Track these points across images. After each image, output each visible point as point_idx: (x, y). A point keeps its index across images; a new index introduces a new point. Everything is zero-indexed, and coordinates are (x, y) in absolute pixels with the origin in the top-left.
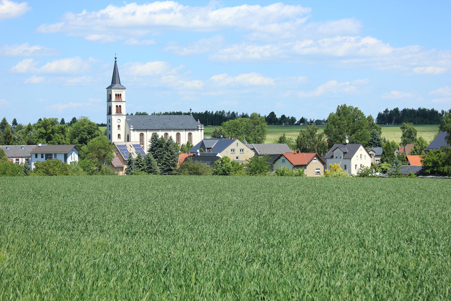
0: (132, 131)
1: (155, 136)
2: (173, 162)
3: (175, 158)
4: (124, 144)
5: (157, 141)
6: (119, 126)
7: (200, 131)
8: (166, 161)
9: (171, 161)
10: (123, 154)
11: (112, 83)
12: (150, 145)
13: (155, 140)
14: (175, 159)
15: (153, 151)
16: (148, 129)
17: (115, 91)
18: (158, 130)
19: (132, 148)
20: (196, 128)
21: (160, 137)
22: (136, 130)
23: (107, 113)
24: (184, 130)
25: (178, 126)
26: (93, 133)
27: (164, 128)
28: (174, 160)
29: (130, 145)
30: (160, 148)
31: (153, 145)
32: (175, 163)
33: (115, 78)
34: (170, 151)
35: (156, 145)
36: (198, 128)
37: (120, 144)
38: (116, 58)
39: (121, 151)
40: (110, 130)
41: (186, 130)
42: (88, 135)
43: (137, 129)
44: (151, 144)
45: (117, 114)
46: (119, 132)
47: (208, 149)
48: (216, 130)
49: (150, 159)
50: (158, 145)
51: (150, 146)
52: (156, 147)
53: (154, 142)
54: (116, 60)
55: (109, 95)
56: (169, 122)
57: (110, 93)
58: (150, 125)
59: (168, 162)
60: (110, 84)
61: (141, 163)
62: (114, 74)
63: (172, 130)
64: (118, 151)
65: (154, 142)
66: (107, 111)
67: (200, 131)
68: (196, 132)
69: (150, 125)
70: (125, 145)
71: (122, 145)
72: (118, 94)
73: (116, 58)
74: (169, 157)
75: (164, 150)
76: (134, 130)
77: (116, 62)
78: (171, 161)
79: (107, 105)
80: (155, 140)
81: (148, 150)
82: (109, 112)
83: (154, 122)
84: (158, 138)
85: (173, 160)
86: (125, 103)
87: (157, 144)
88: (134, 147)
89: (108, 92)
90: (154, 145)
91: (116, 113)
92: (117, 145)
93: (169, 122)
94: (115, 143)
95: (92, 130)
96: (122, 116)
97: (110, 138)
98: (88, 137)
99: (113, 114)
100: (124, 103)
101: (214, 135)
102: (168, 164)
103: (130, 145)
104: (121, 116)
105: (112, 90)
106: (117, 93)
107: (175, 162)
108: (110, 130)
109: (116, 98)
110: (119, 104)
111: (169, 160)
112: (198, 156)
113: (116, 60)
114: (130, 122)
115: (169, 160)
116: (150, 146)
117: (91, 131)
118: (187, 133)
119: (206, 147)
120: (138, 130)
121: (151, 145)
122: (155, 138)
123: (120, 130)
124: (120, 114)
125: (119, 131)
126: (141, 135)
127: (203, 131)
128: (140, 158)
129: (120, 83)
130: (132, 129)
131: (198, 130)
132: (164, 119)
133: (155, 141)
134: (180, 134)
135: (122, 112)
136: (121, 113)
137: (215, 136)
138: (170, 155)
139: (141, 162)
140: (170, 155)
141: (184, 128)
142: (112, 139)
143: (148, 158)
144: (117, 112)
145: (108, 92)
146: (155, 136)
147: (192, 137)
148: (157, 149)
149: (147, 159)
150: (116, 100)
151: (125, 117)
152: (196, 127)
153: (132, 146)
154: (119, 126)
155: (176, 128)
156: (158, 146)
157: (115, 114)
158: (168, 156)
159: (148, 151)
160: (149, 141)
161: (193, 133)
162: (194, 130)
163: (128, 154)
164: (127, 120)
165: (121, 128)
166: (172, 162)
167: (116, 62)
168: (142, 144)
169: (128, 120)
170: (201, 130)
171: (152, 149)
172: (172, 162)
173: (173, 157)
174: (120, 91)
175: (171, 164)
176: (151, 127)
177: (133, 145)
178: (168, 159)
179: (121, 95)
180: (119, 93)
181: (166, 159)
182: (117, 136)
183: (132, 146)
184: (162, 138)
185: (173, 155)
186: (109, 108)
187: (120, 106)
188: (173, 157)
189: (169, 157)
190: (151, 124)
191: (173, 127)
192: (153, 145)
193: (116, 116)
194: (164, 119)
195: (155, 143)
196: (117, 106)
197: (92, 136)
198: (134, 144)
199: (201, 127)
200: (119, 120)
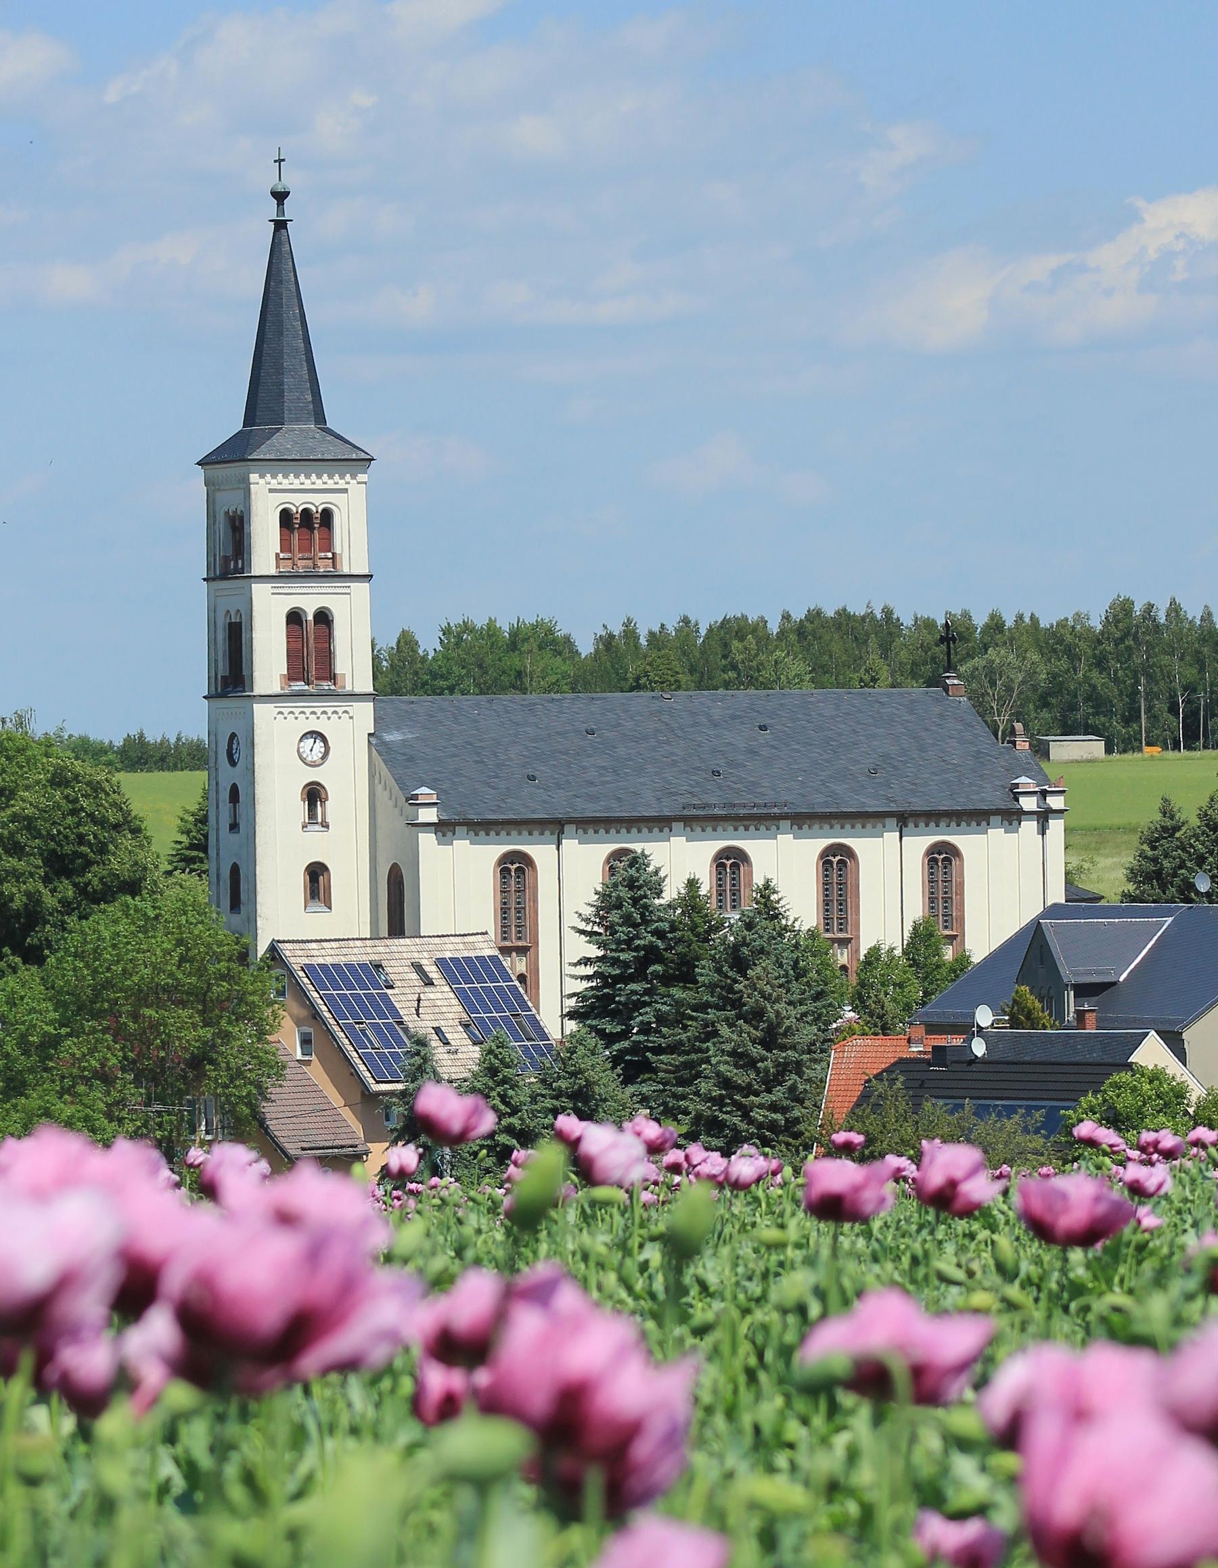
0: (427, 840)
1: (631, 884)
2: (784, 1110)
3: (800, 1074)
4: (365, 959)
5: (646, 922)
6: (314, 795)
7: (1029, 827)
8: (719, 1102)
9: (766, 1098)
10: (357, 1044)
11: (249, 419)
12: (586, 961)
13: (628, 920)
14: (801, 1087)
15: (613, 1015)
16: (571, 821)
17: (274, 484)
18: (661, 824)
19: (430, 994)
20: (999, 800)
21: (672, 890)
22: (461, 830)
23: (213, 678)
24: (891, 822)
25: (839, 788)
26: (89, 863)
27: (714, 800)
28: (793, 1088)
29: (418, 968)
30: (677, 992)
31: (615, 962)
32: (797, 1121)
33: (280, 371)
34: (757, 1015)
35: (643, 963)
36: (1011, 805)
37: (329, 961)
38: (280, 197)
39: (337, 1014)
40: (234, 827)
41: (905, 820)
42: (46, 880)
43: (475, 817)
44: (594, 952)
45: (299, 686)
46: (316, 847)
47: (1083, 991)
48: (1169, 823)
49: (589, 1084)
50: (660, 960)
51: (589, 971)
52: (640, 975)
53: (623, 932)
54: (281, 211)
55: (221, 518)
56: (752, 752)
57: (229, 502)
58: (591, 783)
59: (739, 1106)
60: (238, 426)
61: (514, 1121)
62: (269, 335)
63: (785, 824)
64: (316, 1015)
65: (623, 932)
66: (213, 663)
67: (1029, 827)
68: (996, 834)
69: (591, 783)
70: (378, 966)
71: (350, 966)
72: (306, 512)
73: (280, 197)
74: (749, 1063)
75: (703, 1007)
76: (444, 829)
77: (280, 225)
78: (766, 1098)
79: (212, 610)
80: (628, 920)
81: (572, 1003)
82: (223, 669)
83: (621, 751)
84: (657, 902)
85: (779, 1094)
86: (365, 586)
87: (652, 954)
88: (451, 979)
89: (219, 496)
90: (626, 965)
91: (291, 677)
92: (309, 969)
93: (752, 752)
94: (287, 950)
95: (81, 839)
96: (341, 706)
97: (235, 904)
98: (50, 901)
99: (259, 688)
100: (355, 586)
101: (1155, 860)
102: (734, 1129)
103: (418, 968)
104: (329, 706)
105: (254, 477)
106: (298, 502)
107: (796, 1113)
108: (234, 827)
109: (285, 545)
110: (309, 600)
111: (748, 1090)
112: (975, 1060)
113: (281, 211)
114: (411, 759)
115: (748, 1090)
116: (589, 971)
117: (68, 849)
118: (918, 844)
119: (1068, 974)
120: (481, 828)
121: (599, 959)
122: (635, 901)
123: (325, 825)
124: (326, 685)
125: (315, 835)
126: (505, 872)
127: (1056, 826)
128: (505, 1081)
129: (320, 418)
130: (429, 815)
131: (1012, 817)
132: (715, 725)
133: (635, 926)
134: (848, 852)
135: (341, 666)
136: (332, 677)
137: (1158, 875)
138: (756, 1051)
139: (515, 1111)
140: (756, 1051)
141: (893, 808)
142: (260, 909)
143: (573, 1074)
144: (297, 669)
145: (219, 496)
146: (631, 884)
147: (961, 885)
148: (647, 992)
149: (563, 1084)
150: (286, 568)
151: (365, 713)
152: (993, 798)
153: (433, 972)
154: (314, 795)
155: (819, 802)
156: (658, 968)
157: (276, 689)
158: (741, 1059)
159: (572, 1015)
160: (582, 926)
161: (967, 843)
162: (977, 818)
163: (401, 1043)
164: (388, 738)
165: (332, 809)
166: (773, 1107)
167: (280, 225)
168: (522, 951)
169: (393, 737)
170: (1044, 817)
171: (609, 999)
172: (773, 1107)
173: (783, 1068)
174: (319, 484)
175: (760, 1126)
176: (593, 798)
177: (441, 963)
178: (739, 1089)
179: (327, 516)
180: (317, 502)
181: (726, 1083)
182: (299, 881)
183: (433, 972)
184: (691, 898)
185: (783, 1048)
186: (221, 636)
187: (324, 617)
188: (783, 1068)
189: (749, 1063)
190: (592, 774)
191: (792, 797)
192: (615, 962)
193: (286, 707)
194: (715, 725)
195: (629, 942)
196: (294, 618)
197: (82, 890)
198: (448, 955)
199: (1044, 794)
200: (319, 745)
